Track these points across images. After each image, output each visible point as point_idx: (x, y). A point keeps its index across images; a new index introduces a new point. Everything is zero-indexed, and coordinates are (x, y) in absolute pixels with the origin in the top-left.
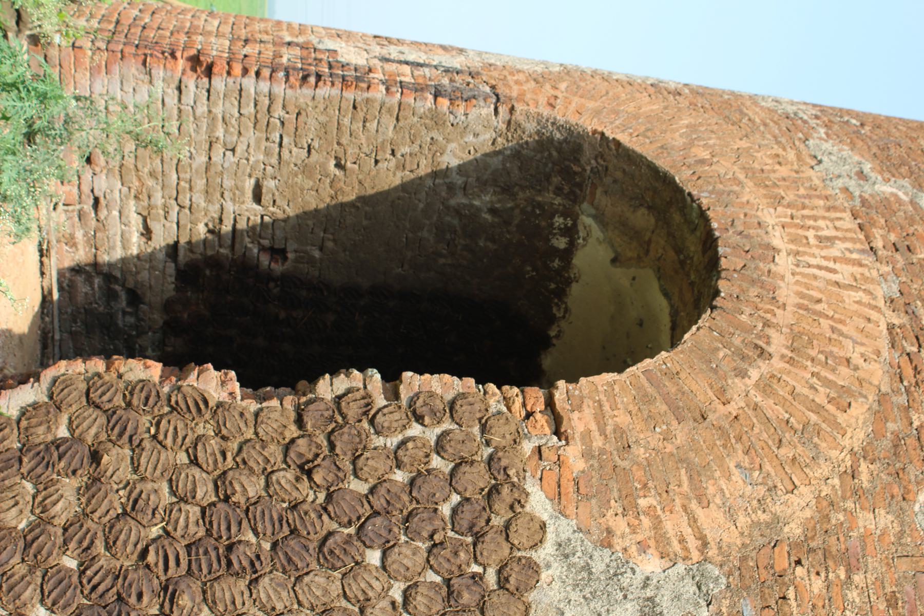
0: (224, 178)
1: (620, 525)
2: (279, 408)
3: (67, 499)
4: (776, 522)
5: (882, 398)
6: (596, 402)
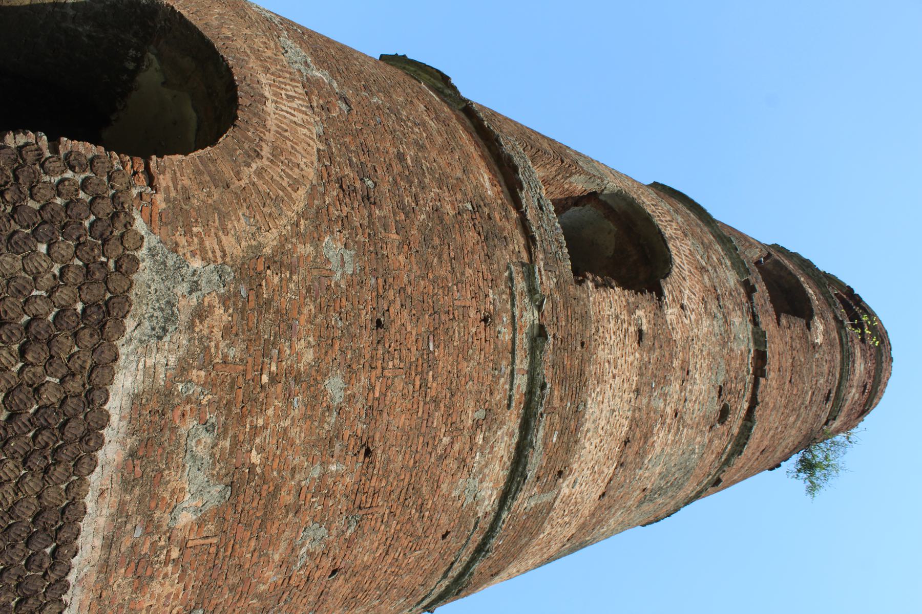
1: (183, 241)
4: (260, 246)
5: (313, 187)
6: (174, 170)
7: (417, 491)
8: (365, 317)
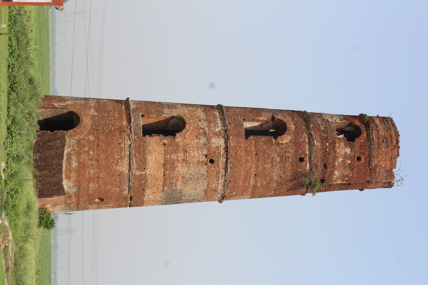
0: (48, 114)
2: (52, 133)
3: (42, 139)
6: (70, 131)
7: (109, 167)
8: (95, 144)
